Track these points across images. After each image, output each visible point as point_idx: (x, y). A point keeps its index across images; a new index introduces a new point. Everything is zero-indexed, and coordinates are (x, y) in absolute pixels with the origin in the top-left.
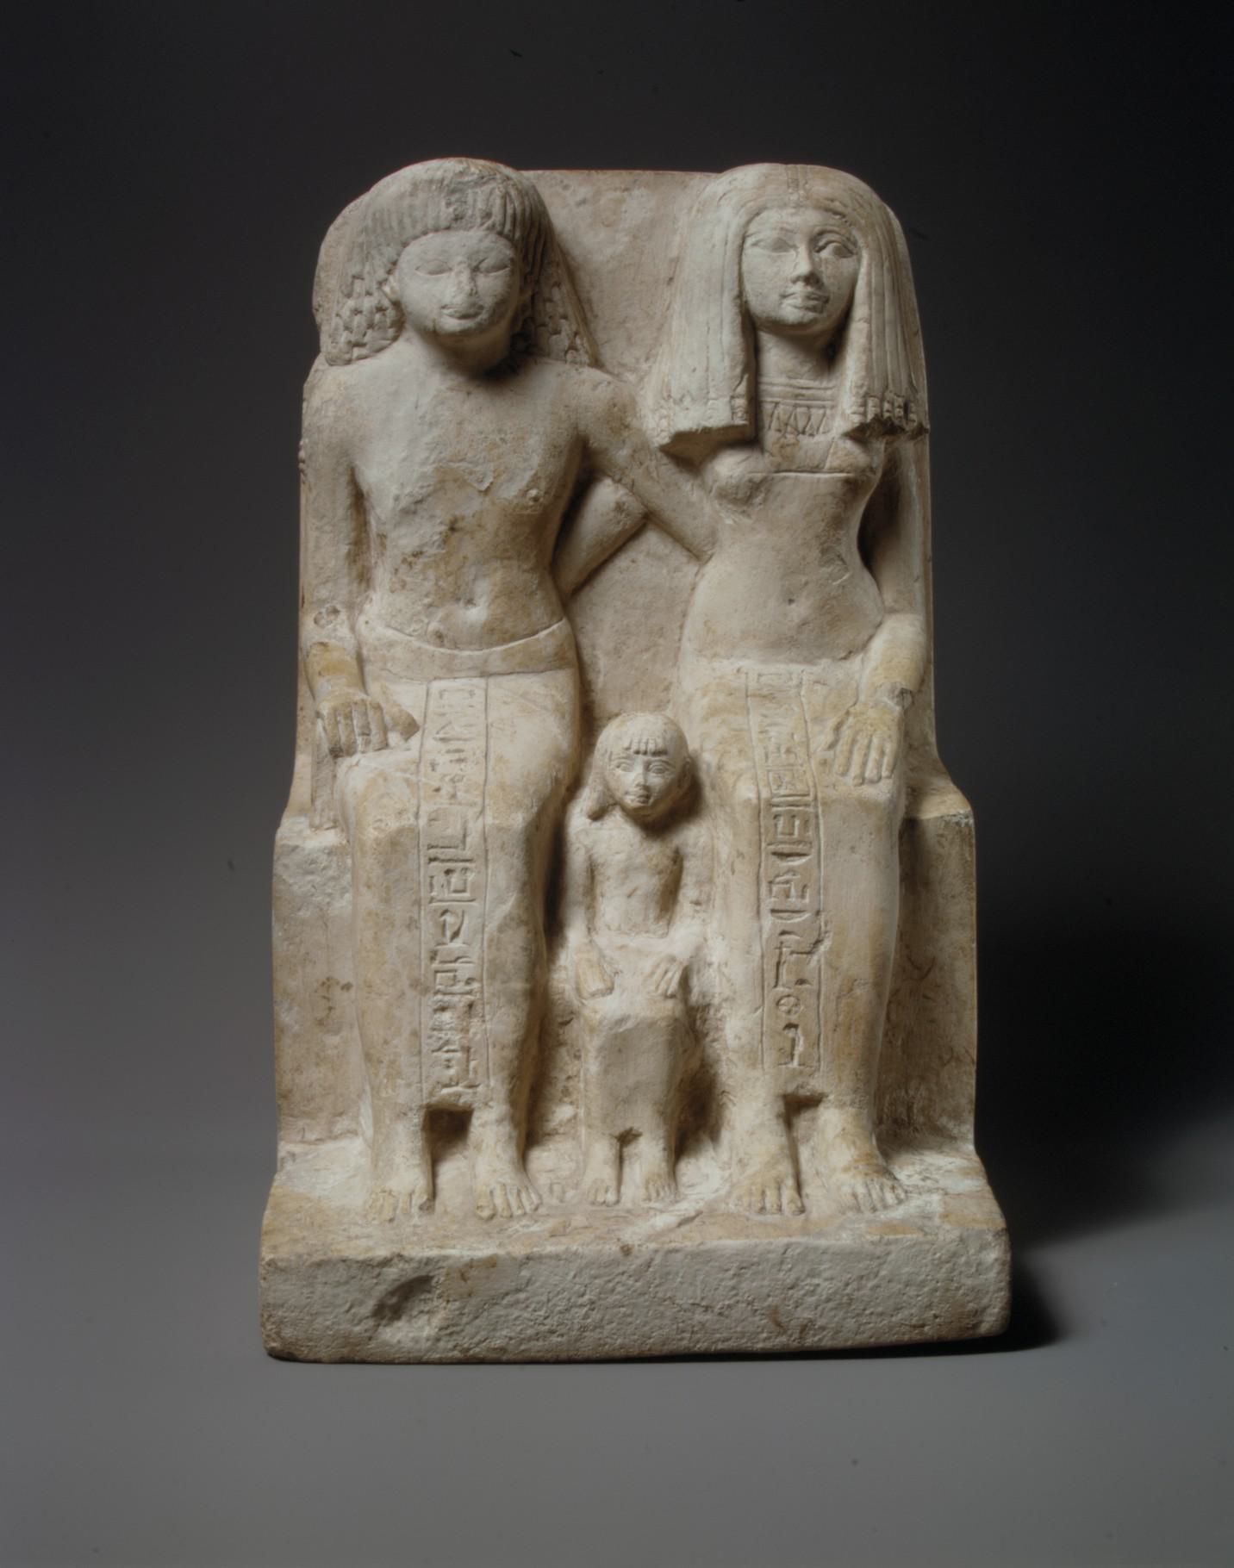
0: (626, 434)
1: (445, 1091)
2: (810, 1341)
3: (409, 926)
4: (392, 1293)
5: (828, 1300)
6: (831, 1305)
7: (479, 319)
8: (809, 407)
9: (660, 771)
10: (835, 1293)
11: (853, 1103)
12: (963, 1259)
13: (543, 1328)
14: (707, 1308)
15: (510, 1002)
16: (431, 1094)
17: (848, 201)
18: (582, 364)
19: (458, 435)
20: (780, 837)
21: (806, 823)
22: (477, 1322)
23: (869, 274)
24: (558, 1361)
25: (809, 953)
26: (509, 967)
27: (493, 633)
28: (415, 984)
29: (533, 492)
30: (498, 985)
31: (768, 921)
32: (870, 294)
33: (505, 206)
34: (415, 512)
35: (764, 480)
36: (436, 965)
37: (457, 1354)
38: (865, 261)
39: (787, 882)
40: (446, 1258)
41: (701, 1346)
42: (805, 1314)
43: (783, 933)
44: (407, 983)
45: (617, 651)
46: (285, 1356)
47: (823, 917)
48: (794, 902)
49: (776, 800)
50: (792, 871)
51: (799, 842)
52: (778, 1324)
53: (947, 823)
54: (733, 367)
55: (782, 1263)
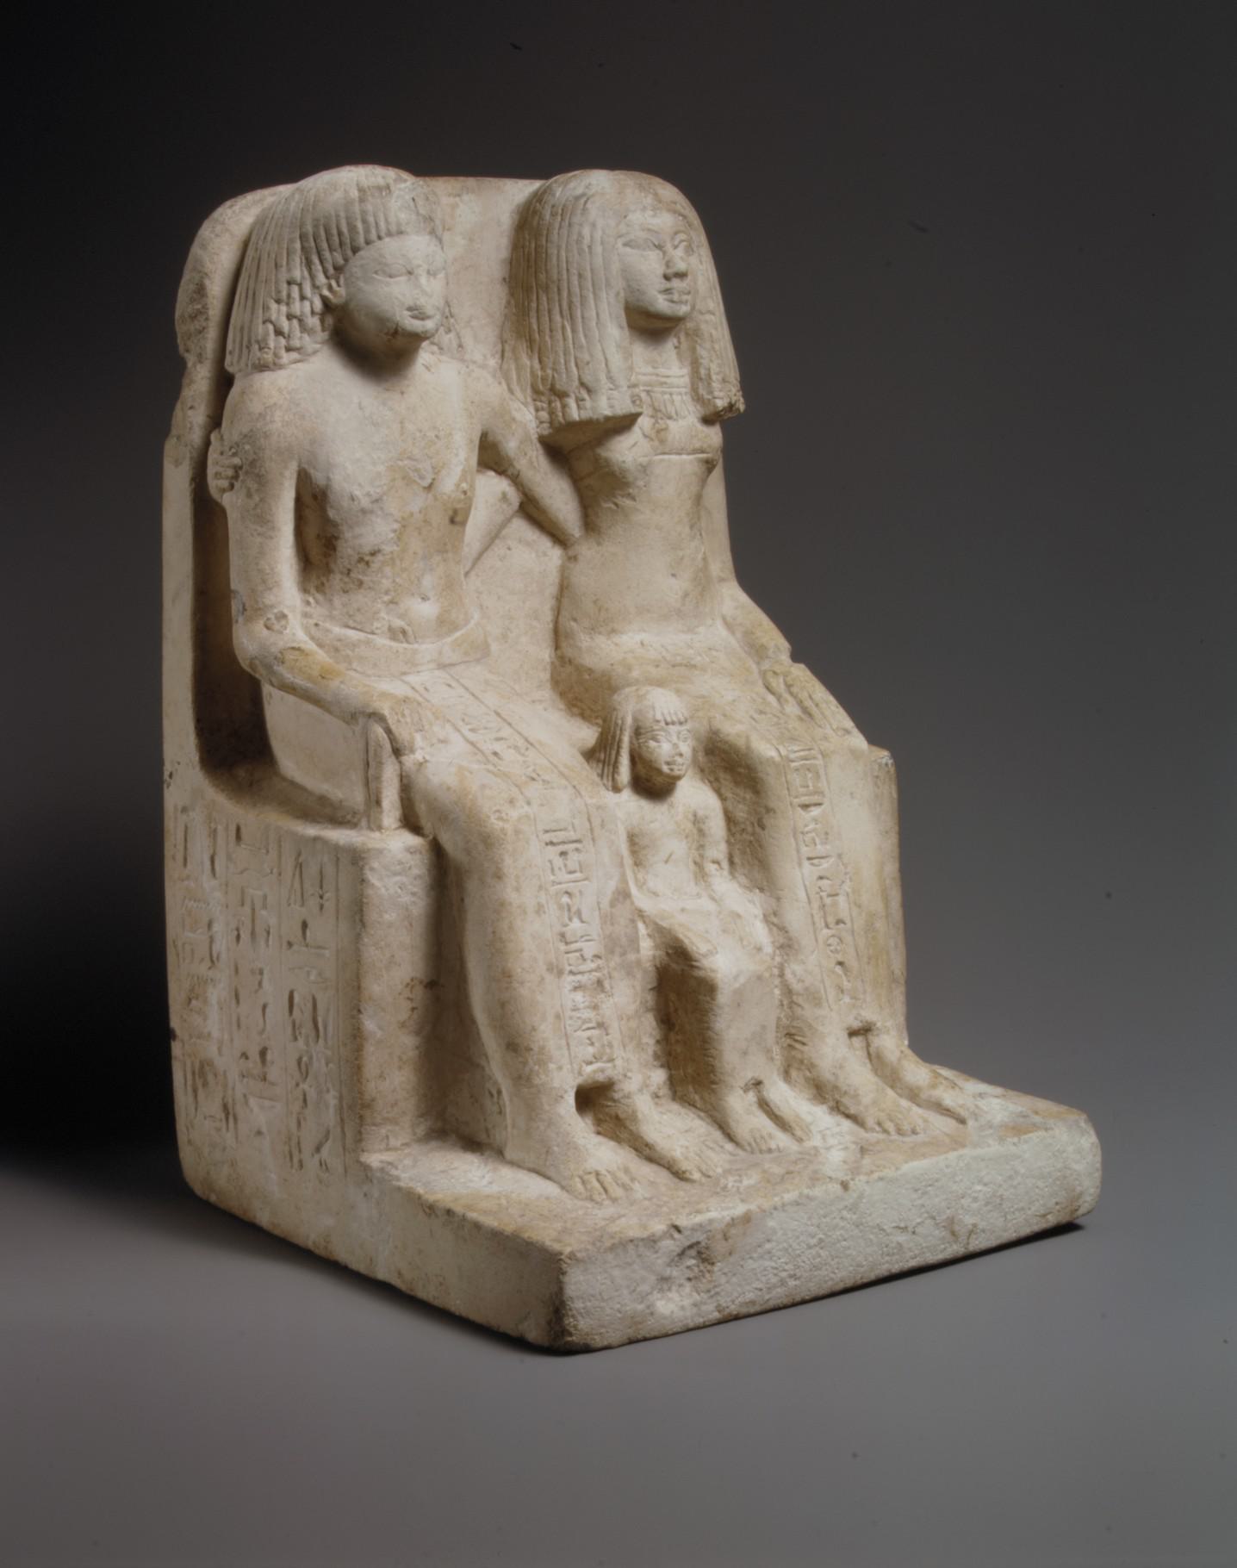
14: (905, 1229)
28: (550, 968)
30: (617, 959)
34: (372, 512)
40: (711, 1221)
43: (821, 878)
45: (504, 637)
48: (820, 849)
50: (815, 820)
52: (953, 1233)
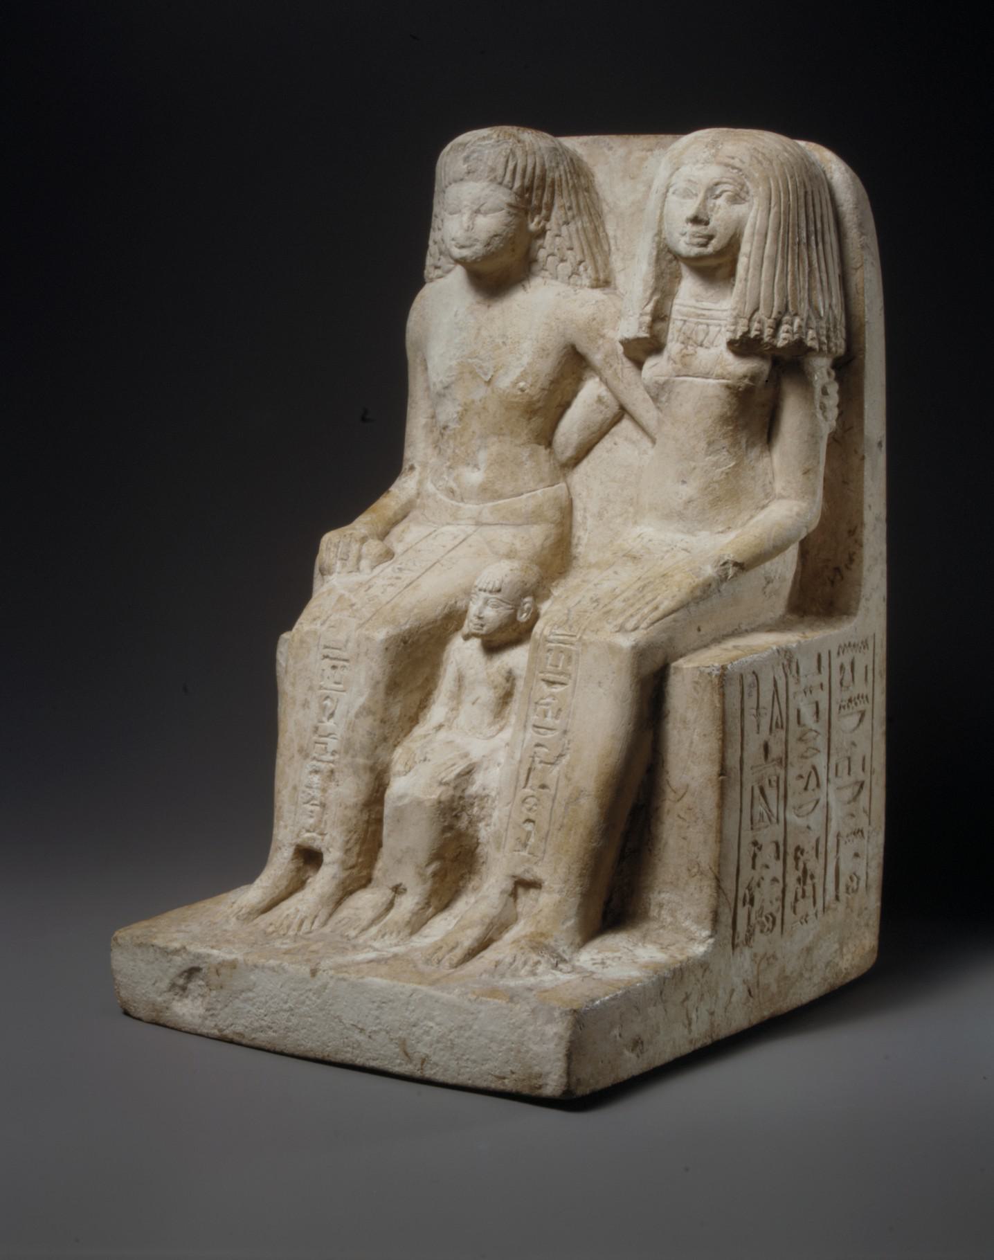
0: (600, 342)
1: (308, 835)
2: (429, 1073)
3: (304, 705)
4: (180, 975)
5: (438, 1042)
6: (440, 1046)
7: (473, 249)
8: (708, 325)
9: (494, 606)
10: (442, 1036)
11: (560, 891)
12: (531, 1028)
13: (264, 1023)
14: (362, 1030)
15: (356, 773)
16: (298, 836)
17: (747, 159)
18: (582, 287)
19: (476, 338)
20: (549, 667)
21: (569, 659)
22: (227, 1010)
23: (756, 218)
24: (268, 1051)
25: (552, 764)
26: (358, 746)
27: (487, 492)
28: (301, 750)
29: (522, 384)
30: (349, 759)
31: (530, 732)
32: (753, 234)
33: (507, 162)
34: (444, 396)
35: (666, 383)
36: (315, 738)
37: (216, 1032)
38: (755, 207)
39: (547, 704)
40: (209, 956)
41: (359, 1061)
42: (423, 1050)
43: (538, 745)
44: (296, 748)
45: (600, 515)
46: (126, 1013)
47: (569, 736)
48: (549, 721)
49: (552, 637)
50: (553, 696)
51: (561, 673)
52: (407, 1054)
53: (701, 673)
54: (645, 291)
55: (408, 1003)
